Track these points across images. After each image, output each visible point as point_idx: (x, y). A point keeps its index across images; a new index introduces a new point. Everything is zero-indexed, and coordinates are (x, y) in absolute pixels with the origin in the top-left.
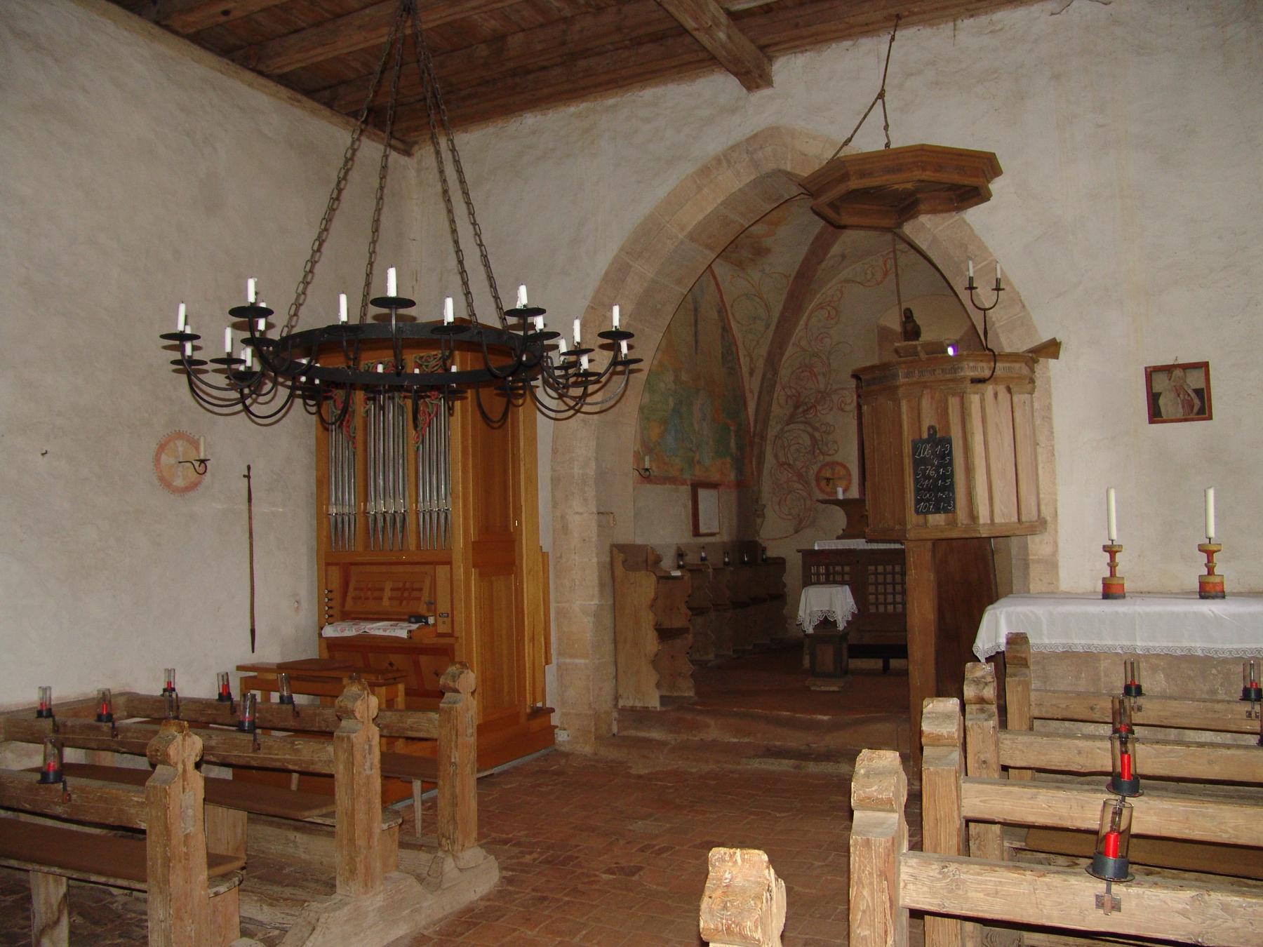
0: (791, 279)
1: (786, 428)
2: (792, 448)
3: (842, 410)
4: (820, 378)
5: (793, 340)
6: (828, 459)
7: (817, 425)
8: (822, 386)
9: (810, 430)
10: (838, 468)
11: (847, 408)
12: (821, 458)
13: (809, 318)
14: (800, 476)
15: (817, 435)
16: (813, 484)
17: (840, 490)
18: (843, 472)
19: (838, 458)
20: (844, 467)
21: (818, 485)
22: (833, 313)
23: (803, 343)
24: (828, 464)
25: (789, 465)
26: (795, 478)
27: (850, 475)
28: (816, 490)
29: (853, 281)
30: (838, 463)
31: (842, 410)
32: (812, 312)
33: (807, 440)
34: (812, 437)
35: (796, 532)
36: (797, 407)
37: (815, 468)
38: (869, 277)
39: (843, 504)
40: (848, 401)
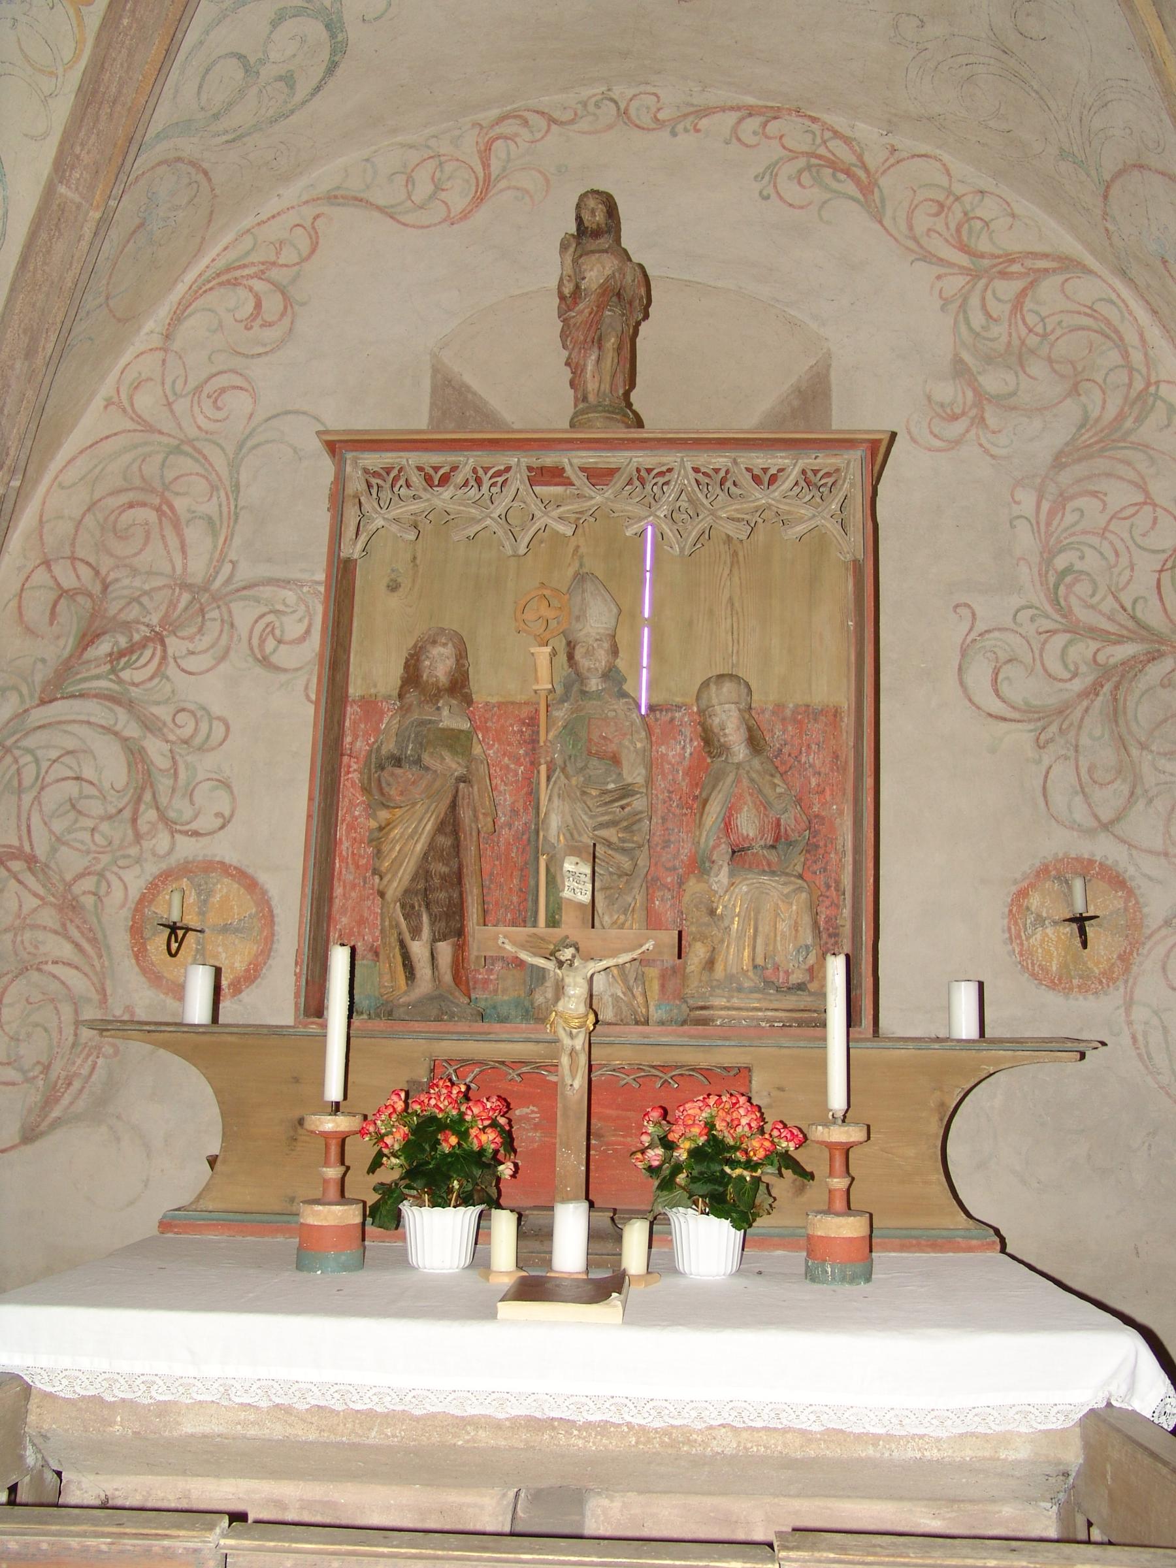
1: (39, 715)
2: (53, 797)
3: (265, 662)
4: (192, 534)
5: (106, 389)
6: (187, 848)
7: (163, 712)
8: (198, 568)
9: (133, 730)
10: (224, 889)
11: (284, 656)
12: (162, 841)
13: (178, 317)
14: (70, 907)
15: (155, 748)
16: (120, 941)
17: (199, 984)
18: (241, 906)
19: (223, 849)
20: (250, 884)
21: (140, 954)
22: (273, 305)
23: (145, 402)
24: (186, 869)
25: (31, 860)
26: (49, 917)
27: (269, 918)
28: (128, 969)
29: (359, 201)
30: (225, 869)
31: (265, 662)
32: (196, 292)
33: (111, 768)
34: (135, 755)
35: (29, 1136)
36: (88, 639)
37: (136, 881)
38: (423, 189)
39: (214, 1046)
40: (293, 628)
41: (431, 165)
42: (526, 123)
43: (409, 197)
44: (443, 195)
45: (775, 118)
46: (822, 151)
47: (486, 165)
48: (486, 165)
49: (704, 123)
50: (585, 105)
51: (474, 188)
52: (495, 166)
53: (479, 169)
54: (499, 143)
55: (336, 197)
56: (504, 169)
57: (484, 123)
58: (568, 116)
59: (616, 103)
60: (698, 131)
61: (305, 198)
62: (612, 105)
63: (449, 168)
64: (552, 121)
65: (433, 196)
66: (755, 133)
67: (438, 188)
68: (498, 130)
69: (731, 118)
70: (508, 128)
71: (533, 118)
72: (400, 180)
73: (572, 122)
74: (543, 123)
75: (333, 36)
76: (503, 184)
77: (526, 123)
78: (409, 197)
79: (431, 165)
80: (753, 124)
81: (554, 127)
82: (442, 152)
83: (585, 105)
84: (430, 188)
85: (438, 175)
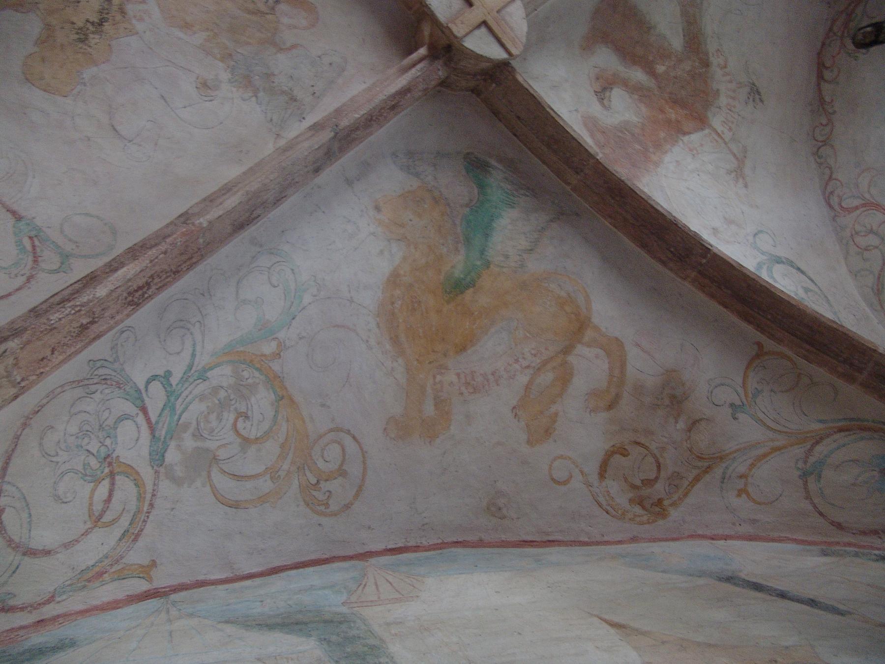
0: (770, 344)
38: (873, 240)
41: (858, 239)
42: (832, 193)
43: (876, 247)
44: (874, 228)
45: (823, 64)
46: (839, 34)
47: (857, 208)
48: (857, 208)
49: (827, 99)
50: (821, 164)
51: (870, 212)
52: (856, 202)
53: (858, 212)
54: (843, 204)
55: (878, 290)
56: (858, 197)
57: (833, 214)
58: (827, 171)
59: (819, 148)
60: (832, 101)
61: (879, 308)
62: (821, 150)
63: (858, 228)
64: (830, 178)
65: (876, 234)
66: (832, 71)
67: (871, 231)
68: (837, 207)
69: (825, 87)
70: (835, 201)
71: (829, 189)
72: (866, 254)
73: (830, 168)
74: (832, 183)
75: (783, 262)
76: (867, 196)
77: (832, 193)
78: (876, 247)
79: (858, 239)
80: (827, 75)
81: (834, 176)
82: (849, 234)
83: (821, 164)
84: (871, 236)
85: (863, 234)
